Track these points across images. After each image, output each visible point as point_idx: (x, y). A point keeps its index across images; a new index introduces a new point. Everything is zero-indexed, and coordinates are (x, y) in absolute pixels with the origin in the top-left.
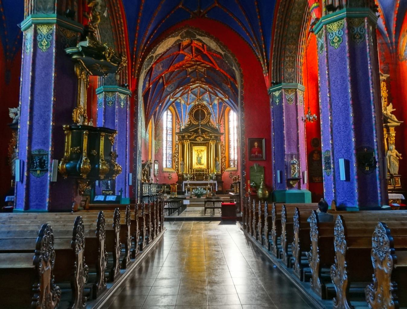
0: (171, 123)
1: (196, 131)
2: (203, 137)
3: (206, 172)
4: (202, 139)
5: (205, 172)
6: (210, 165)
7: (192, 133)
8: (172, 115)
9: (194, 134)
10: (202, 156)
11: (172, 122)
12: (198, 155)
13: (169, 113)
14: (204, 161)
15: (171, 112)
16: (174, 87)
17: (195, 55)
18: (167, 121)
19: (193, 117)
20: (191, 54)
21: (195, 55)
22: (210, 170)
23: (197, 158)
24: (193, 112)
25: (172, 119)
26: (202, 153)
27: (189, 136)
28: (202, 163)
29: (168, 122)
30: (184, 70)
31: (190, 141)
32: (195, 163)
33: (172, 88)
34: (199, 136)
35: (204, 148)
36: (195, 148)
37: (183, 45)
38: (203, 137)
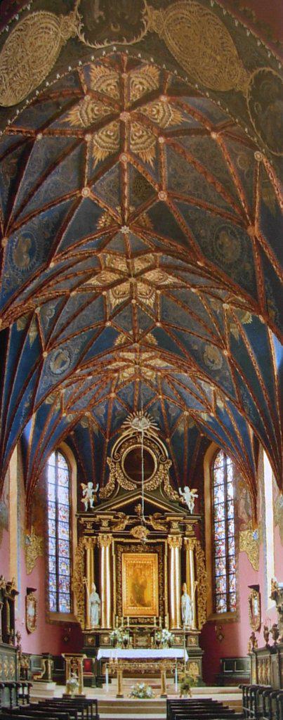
0: (67, 490)
1: (129, 510)
2: (150, 528)
3: (158, 624)
4: (147, 532)
5: (155, 626)
6: (166, 607)
7: (120, 514)
8: (70, 470)
9: (124, 518)
10: (146, 581)
11: (70, 488)
12: (136, 579)
13: (62, 464)
14: (152, 594)
15: (67, 461)
16: (69, 359)
17: (132, 209)
18: (56, 485)
19: (121, 468)
20: (118, 209)
21: (132, 209)
22: (167, 618)
23: (134, 586)
24: (121, 456)
25: (70, 480)
26: (147, 573)
27: (111, 524)
28: (146, 602)
29: (59, 488)
30: (95, 297)
31: (113, 536)
32: (129, 602)
33: (64, 363)
34: (138, 524)
35: (151, 558)
36: (128, 559)
37: (92, 160)
38: (150, 528)
